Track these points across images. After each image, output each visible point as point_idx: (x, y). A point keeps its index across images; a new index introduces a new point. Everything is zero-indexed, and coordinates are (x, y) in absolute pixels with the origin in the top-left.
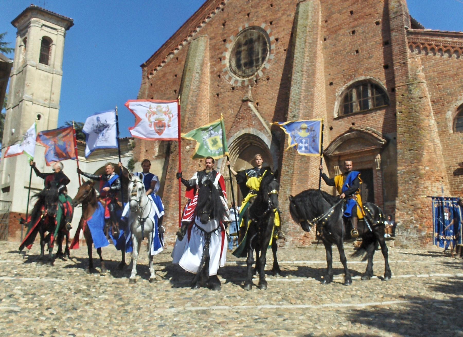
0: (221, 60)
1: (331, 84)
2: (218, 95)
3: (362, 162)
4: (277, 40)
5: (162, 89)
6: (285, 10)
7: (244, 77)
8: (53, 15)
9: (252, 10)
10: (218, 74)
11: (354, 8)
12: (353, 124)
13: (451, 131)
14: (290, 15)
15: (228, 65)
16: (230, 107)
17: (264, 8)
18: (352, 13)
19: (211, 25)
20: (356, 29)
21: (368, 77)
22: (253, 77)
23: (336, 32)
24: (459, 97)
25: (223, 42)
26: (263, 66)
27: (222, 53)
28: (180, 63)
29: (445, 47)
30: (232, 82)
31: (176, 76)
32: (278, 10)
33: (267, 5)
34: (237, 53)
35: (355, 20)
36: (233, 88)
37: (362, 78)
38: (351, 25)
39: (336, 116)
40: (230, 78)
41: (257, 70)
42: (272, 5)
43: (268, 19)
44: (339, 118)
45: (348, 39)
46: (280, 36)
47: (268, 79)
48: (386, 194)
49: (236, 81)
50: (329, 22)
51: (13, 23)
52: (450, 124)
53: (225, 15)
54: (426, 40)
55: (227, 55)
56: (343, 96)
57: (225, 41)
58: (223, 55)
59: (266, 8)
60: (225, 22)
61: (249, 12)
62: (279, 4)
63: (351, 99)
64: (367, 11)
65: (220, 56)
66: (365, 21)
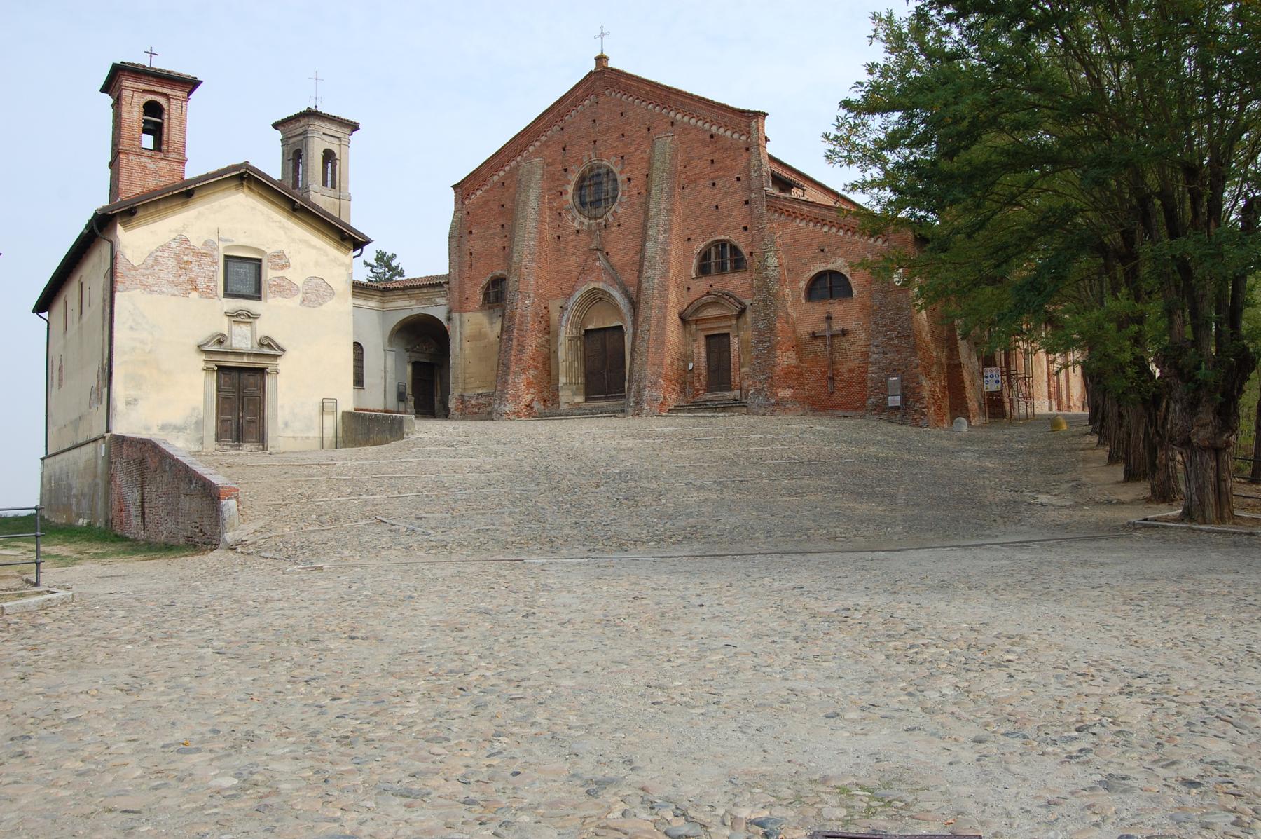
0: (561, 194)
1: (689, 239)
2: (559, 237)
3: (719, 327)
4: (629, 179)
5: (485, 220)
6: (638, 144)
7: (590, 219)
8: (330, 119)
9: (600, 138)
10: (559, 211)
11: (715, 158)
12: (711, 286)
13: (803, 301)
14: (646, 151)
15: (571, 201)
16: (574, 254)
17: (614, 136)
18: (712, 161)
19: (547, 147)
20: (715, 181)
21: (727, 237)
22: (601, 220)
23: (695, 181)
24: (812, 268)
25: (563, 172)
26: (613, 208)
27: (563, 185)
28: (508, 191)
29: (802, 215)
30: (575, 225)
31: (503, 206)
32: (631, 144)
33: (619, 134)
34: (580, 187)
35: (716, 171)
36: (578, 231)
37: (722, 237)
38: (712, 175)
39: (694, 276)
40: (574, 219)
41: (606, 213)
42: (623, 135)
43: (619, 151)
44: (697, 278)
45: (707, 192)
46: (633, 176)
47: (619, 226)
48: (742, 361)
49: (581, 223)
50: (688, 168)
51: (276, 126)
52: (803, 294)
53: (566, 137)
54: (784, 205)
55: (570, 189)
56: (701, 255)
57: (566, 170)
58: (564, 188)
59: (617, 138)
60: (566, 146)
61: (595, 139)
62: (632, 135)
63: (710, 259)
64: (729, 163)
65: (560, 189)
66: (726, 173)
